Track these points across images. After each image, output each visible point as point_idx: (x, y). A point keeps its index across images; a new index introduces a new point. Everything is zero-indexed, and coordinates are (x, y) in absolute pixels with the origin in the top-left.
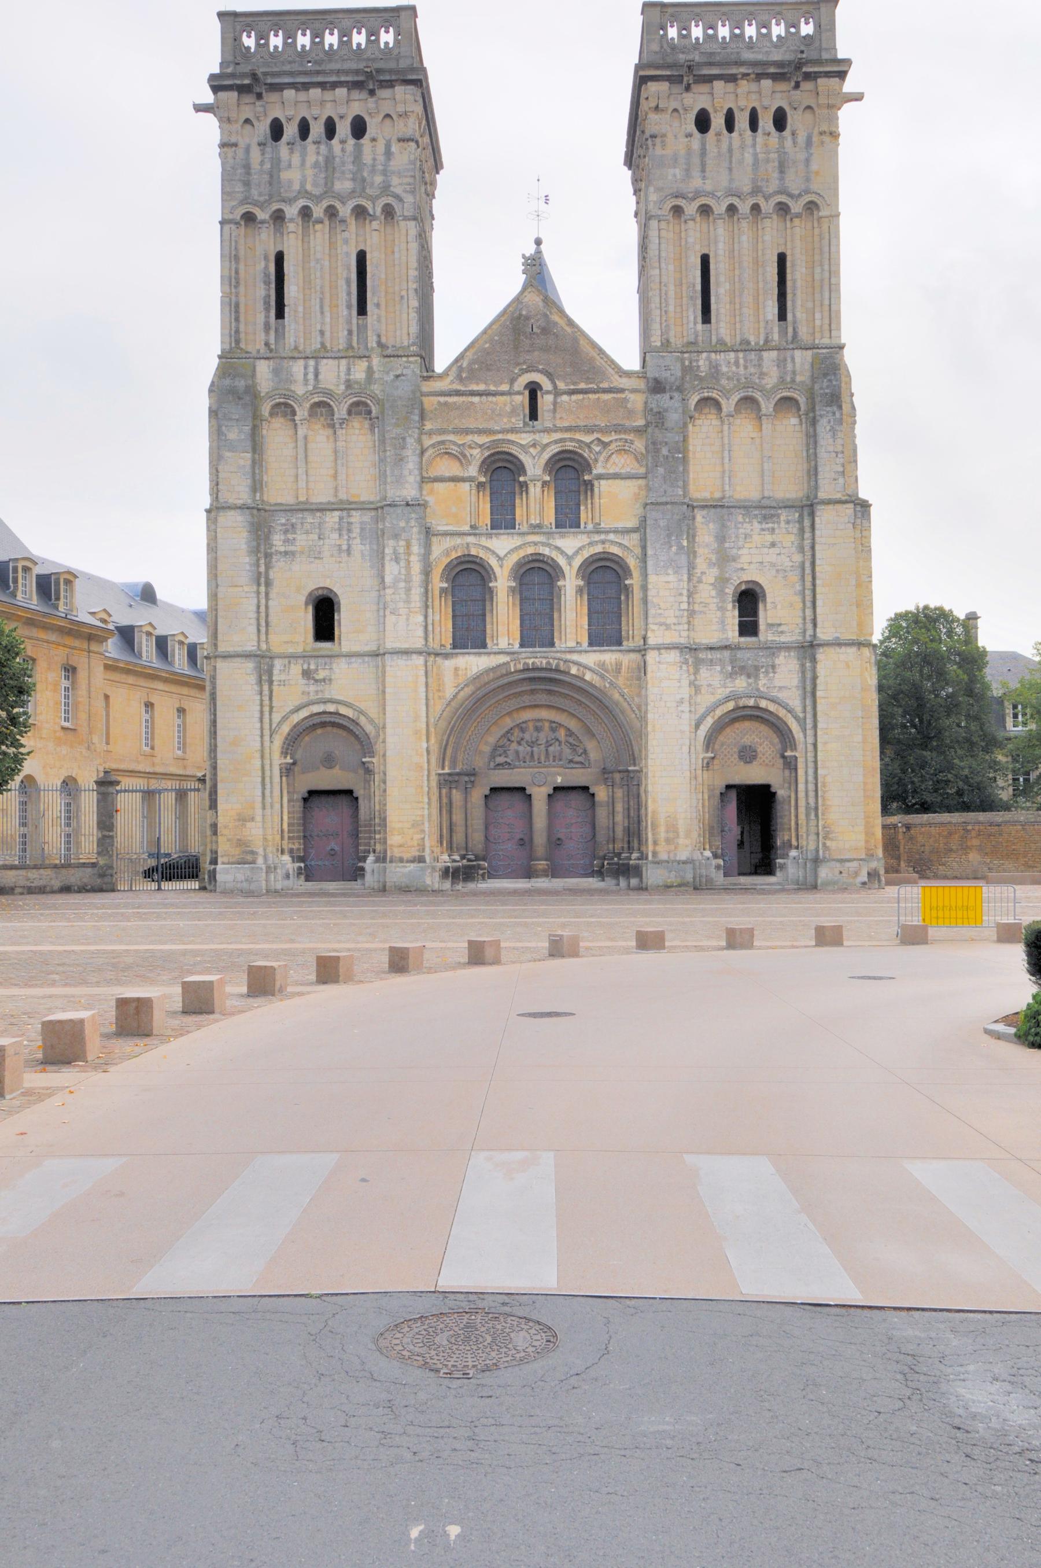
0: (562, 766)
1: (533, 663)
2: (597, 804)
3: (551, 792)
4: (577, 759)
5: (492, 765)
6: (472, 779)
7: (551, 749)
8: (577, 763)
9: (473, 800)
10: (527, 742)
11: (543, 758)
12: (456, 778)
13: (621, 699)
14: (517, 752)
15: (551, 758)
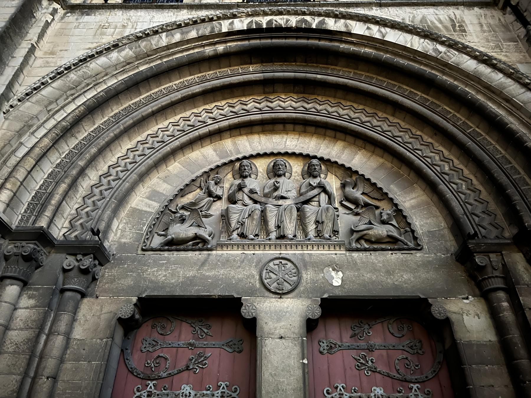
0: (340, 245)
1: (270, 22)
2: (466, 354)
3: (317, 312)
4: (381, 230)
5: (157, 241)
6: (87, 262)
7: (310, 209)
8: (379, 241)
9: (78, 333)
10: (252, 191)
11: (290, 228)
12: (29, 247)
13: (484, 70)
14: (225, 216)
15: (311, 228)
